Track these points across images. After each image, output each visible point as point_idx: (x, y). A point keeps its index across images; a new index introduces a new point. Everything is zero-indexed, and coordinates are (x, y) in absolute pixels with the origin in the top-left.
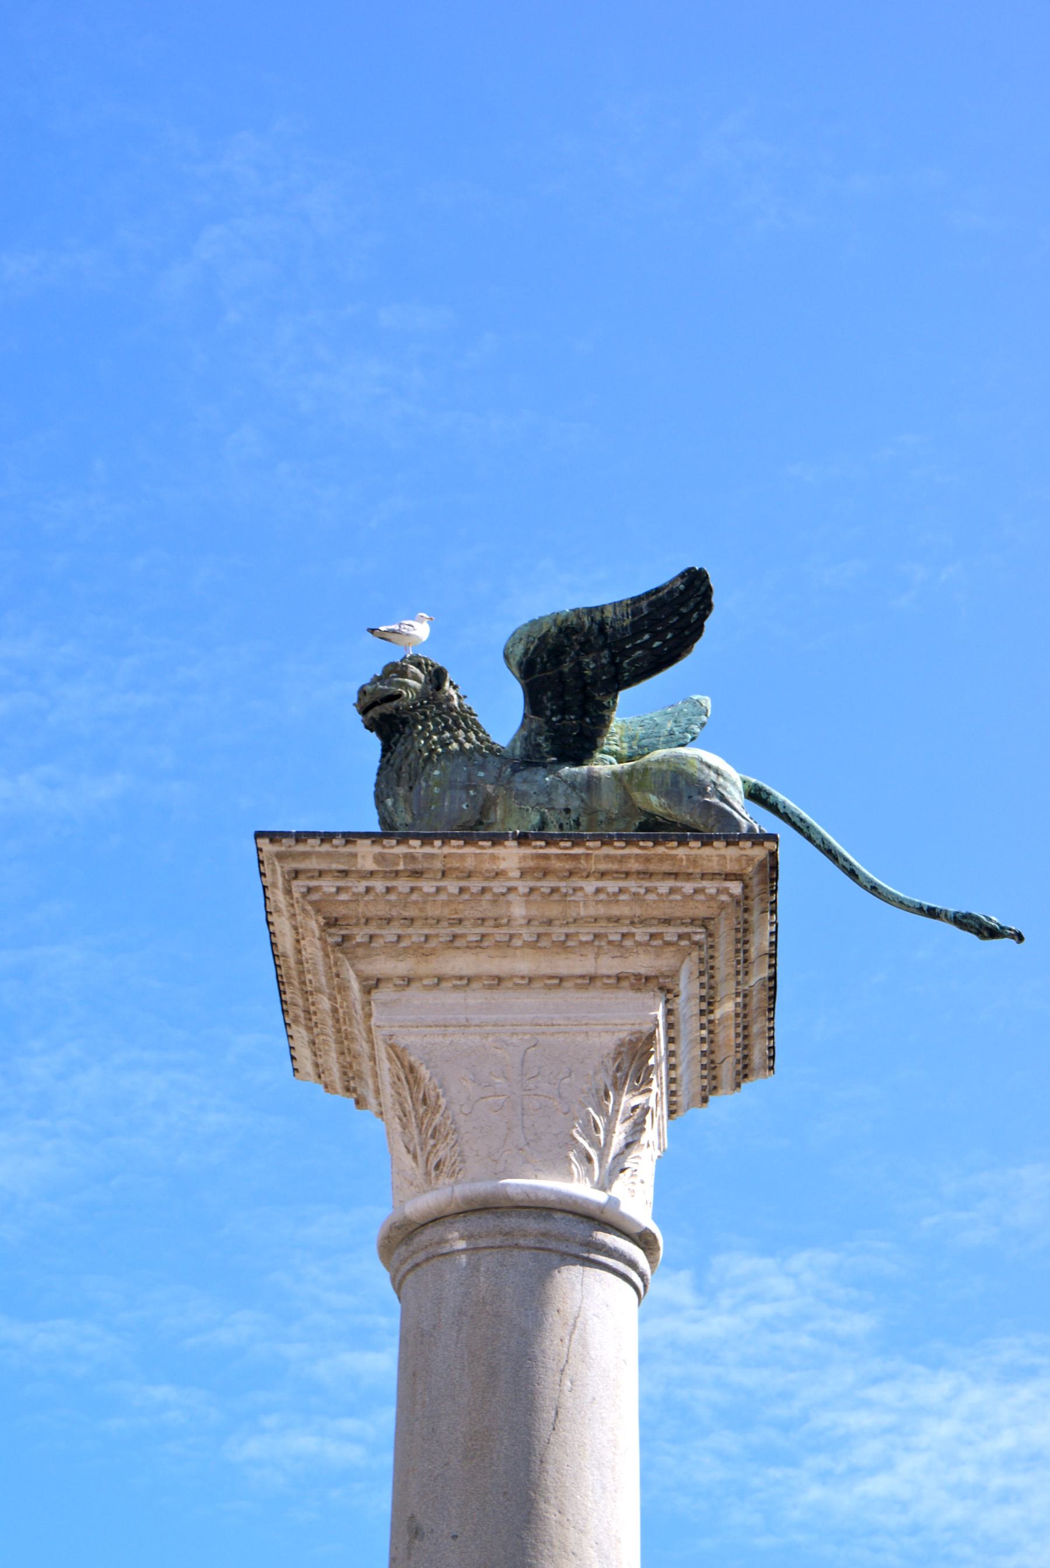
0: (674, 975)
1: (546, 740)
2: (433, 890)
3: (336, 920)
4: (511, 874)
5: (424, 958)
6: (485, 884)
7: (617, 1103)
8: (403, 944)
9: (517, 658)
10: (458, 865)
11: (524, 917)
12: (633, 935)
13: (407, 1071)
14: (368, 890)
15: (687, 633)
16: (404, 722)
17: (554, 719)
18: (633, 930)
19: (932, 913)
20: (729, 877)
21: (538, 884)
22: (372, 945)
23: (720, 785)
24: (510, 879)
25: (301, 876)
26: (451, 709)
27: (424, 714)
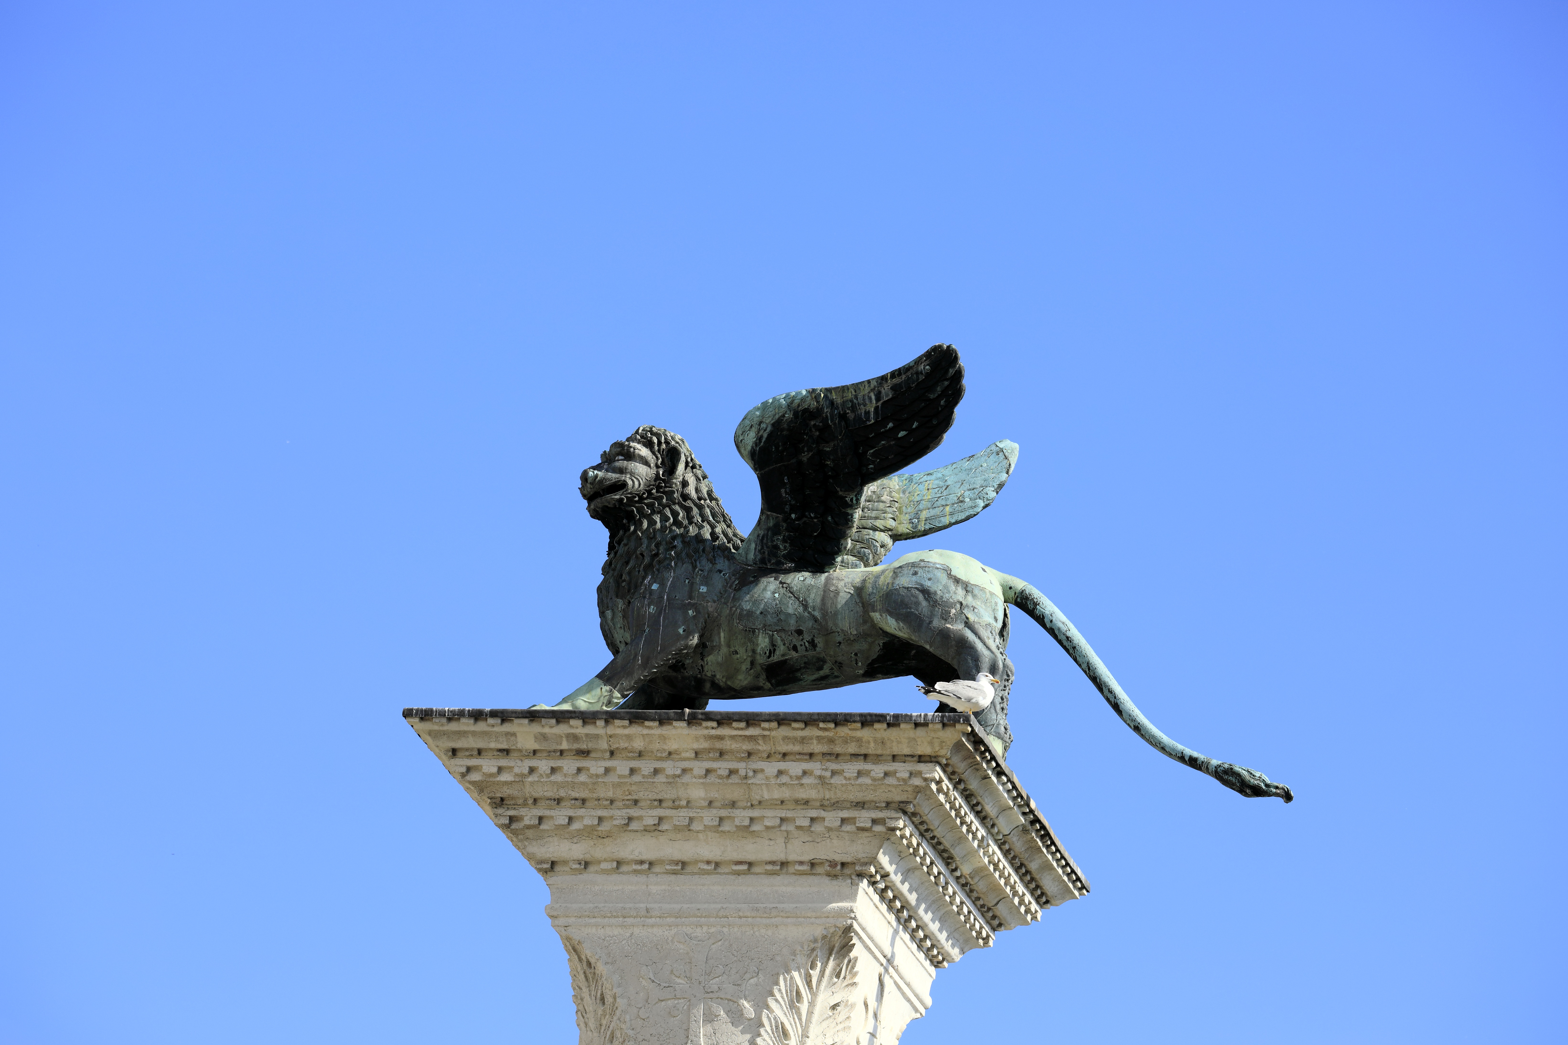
0: (873, 860)
1: (784, 541)
2: (601, 771)
3: (502, 799)
5: (601, 840)
6: (658, 765)
7: (812, 1004)
8: (576, 826)
9: (749, 448)
10: (626, 745)
11: (704, 799)
12: (823, 819)
13: (585, 964)
14: (532, 770)
15: (935, 422)
16: (630, 516)
17: (793, 516)
19: (1193, 763)
20: (921, 759)
22: (542, 827)
23: (967, 606)
24: (685, 759)
25: (459, 754)
26: (685, 497)
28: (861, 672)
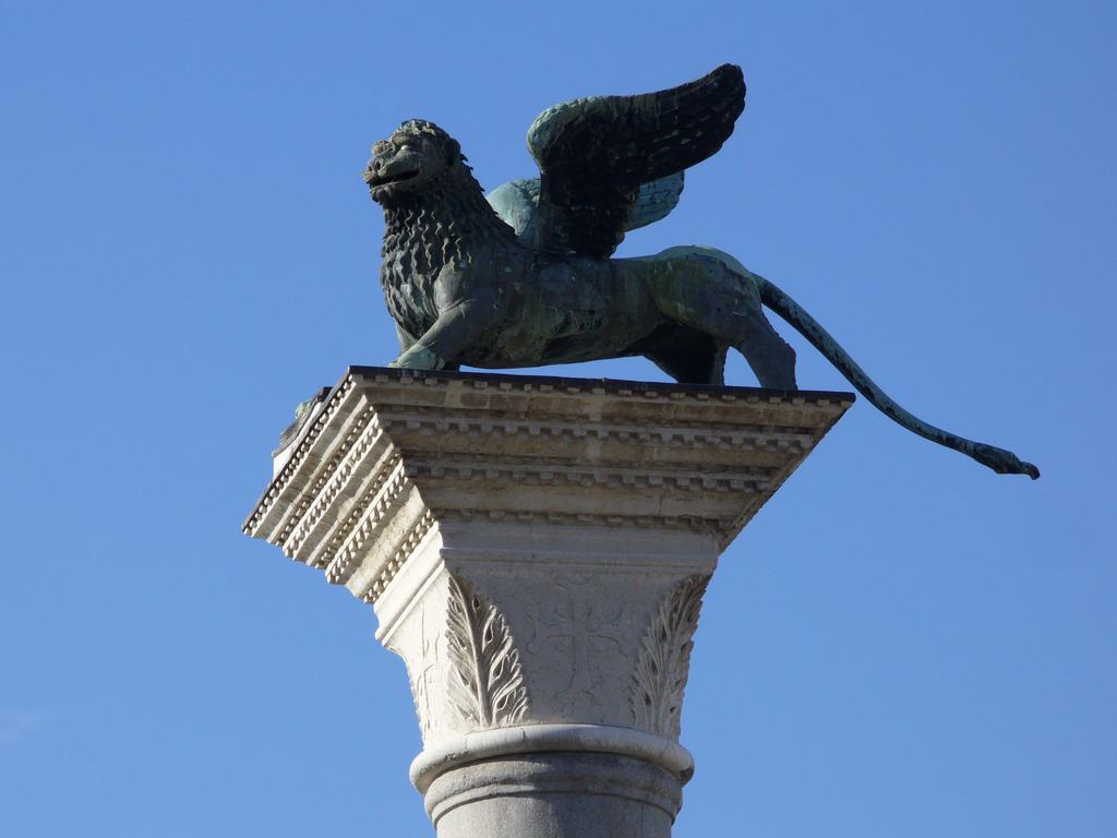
3: (414, 451)
4: (592, 419)
6: (566, 426)
17: (573, 209)
18: (702, 476)
19: (951, 442)
21: (617, 429)
24: (591, 423)
27: (440, 193)
28: (619, 350)
